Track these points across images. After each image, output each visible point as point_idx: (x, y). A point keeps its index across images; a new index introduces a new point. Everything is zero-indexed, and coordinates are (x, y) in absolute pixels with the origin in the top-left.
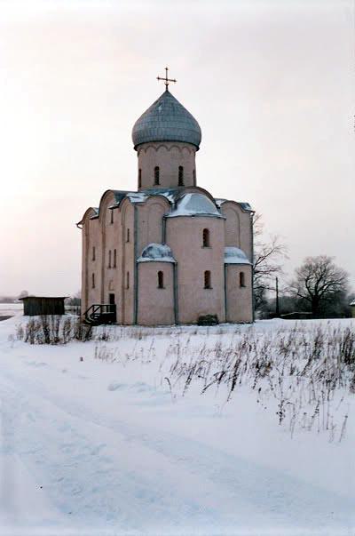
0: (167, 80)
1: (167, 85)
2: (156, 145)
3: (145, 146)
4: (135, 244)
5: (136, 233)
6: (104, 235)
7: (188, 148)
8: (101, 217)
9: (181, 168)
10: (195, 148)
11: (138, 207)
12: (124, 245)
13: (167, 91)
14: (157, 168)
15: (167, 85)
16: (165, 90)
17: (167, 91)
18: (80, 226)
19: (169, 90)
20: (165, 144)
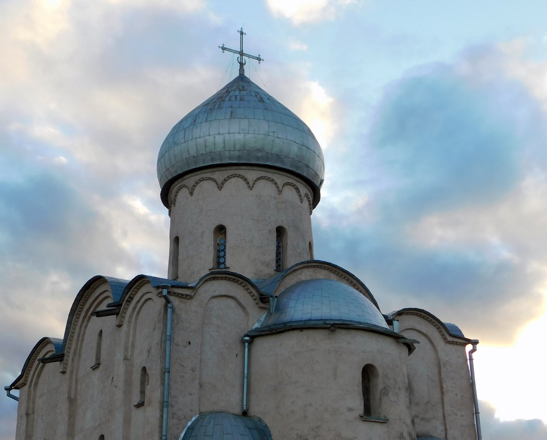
0: (241, 53)
1: (242, 65)
2: (219, 175)
3: (190, 180)
4: (164, 404)
5: (165, 371)
6: (72, 401)
7: (297, 189)
8: (69, 357)
9: (280, 231)
10: (304, 190)
11: (172, 298)
12: (127, 421)
13: (242, 79)
14: (221, 230)
15: (242, 65)
16: (237, 74)
17: (242, 79)
18: (15, 393)
19: (247, 74)
20: (243, 172)
